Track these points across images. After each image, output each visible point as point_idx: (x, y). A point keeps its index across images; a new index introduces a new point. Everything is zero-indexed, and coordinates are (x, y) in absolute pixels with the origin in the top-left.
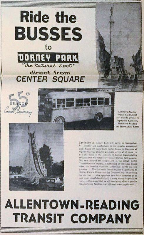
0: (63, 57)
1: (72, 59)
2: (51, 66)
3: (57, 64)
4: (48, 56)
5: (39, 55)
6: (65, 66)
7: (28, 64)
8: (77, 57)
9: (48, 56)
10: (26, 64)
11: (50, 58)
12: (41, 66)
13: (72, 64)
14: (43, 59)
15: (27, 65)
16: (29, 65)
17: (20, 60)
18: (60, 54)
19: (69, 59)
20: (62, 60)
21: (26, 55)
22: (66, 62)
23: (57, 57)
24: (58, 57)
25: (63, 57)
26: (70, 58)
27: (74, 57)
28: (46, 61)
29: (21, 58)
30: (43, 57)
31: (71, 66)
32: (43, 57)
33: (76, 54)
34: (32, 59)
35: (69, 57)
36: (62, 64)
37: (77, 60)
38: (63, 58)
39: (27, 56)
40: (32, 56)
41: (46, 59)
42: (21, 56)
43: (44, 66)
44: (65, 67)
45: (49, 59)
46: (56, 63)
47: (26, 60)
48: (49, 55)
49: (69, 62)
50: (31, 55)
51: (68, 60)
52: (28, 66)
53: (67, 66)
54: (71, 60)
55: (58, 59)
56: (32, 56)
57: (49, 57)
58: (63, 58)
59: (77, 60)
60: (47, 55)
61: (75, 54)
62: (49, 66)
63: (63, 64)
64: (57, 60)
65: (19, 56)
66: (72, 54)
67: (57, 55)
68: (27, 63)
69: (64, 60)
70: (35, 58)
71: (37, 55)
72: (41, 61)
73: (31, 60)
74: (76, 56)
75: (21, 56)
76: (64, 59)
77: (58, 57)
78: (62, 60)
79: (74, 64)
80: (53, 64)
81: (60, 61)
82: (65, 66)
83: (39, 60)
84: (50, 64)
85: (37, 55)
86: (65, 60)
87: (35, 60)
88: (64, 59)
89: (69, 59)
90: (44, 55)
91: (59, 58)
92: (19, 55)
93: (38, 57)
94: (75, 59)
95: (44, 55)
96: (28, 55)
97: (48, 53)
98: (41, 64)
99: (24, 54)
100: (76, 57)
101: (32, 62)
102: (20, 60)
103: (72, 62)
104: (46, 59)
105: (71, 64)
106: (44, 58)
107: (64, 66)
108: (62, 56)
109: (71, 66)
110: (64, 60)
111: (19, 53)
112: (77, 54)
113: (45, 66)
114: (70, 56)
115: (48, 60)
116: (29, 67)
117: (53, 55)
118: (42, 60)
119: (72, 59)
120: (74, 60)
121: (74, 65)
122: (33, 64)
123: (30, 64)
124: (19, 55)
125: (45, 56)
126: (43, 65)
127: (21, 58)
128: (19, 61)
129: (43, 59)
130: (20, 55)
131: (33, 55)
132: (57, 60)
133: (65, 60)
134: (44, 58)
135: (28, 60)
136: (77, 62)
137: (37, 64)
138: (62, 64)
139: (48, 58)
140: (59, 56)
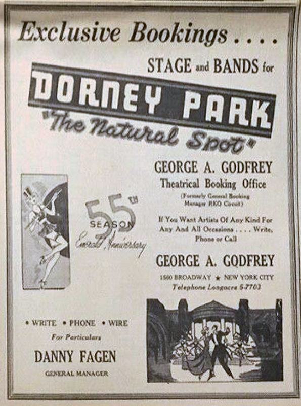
0: (215, 104)
1: (248, 116)
2: (159, 139)
3: (185, 134)
4: (153, 95)
5: (116, 86)
6: (213, 144)
7: (66, 115)
8: (270, 112)
9: (153, 95)
10: (59, 116)
12: (119, 130)
13: (247, 138)
14: (132, 103)
16: (69, 122)
17: (38, 95)
18: (205, 92)
19: (237, 117)
20: (208, 118)
21: (63, 79)
22: (224, 125)
24: (193, 101)
25: (215, 104)
26: (242, 112)
27: (259, 111)
29: (43, 91)
30: (133, 93)
32: (133, 93)
33: (266, 101)
34: (87, 96)
35: (238, 106)
36: (204, 135)
38: (215, 108)
40: (88, 87)
41: (142, 105)
42: (44, 81)
44: (213, 148)
46: (180, 129)
47: (61, 98)
48: (159, 90)
50: (84, 82)
51: (232, 121)
54: (243, 122)
55: (191, 110)
56: (88, 87)
57: (157, 100)
58: (215, 108)
60: (149, 89)
62: (153, 136)
63: (211, 134)
64: (186, 115)
66: (250, 97)
67: (189, 95)
68: (62, 112)
69: (214, 119)
70: (99, 96)
72: (121, 111)
73: (82, 101)
74: (266, 105)
75: (44, 81)
76: (214, 114)
77: (193, 101)
78: (208, 118)
80: (167, 129)
82: (213, 144)
83: (115, 105)
84: (155, 127)
85: (107, 85)
86: (219, 119)
88: (214, 114)
89: (237, 117)
90: (136, 88)
91: (197, 105)
93: (111, 90)
94: (259, 120)
96: (71, 81)
97: (154, 83)
98: (120, 125)
101: (87, 108)
103: (248, 130)
104: (142, 105)
105: (244, 136)
106: (135, 98)
108: (211, 99)
109: (238, 147)
110: (214, 119)
113: (133, 132)
114: (243, 103)
115: (151, 110)
116: (67, 128)
117: (173, 94)
119: (248, 116)
120: (254, 124)
121: (252, 143)
122: (86, 118)
123: (74, 117)
125: (141, 94)
127: (43, 91)
128: (33, 101)
129: (132, 103)
130: (39, 76)
131: (93, 83)
132: (186, 115)
133: (219, 119)
134: (135, 98)
135: (68, 98)
136: (267, 133)
137: (105, 122)
138: (204, 135)
139: (153, 102)
140: (198, 97)
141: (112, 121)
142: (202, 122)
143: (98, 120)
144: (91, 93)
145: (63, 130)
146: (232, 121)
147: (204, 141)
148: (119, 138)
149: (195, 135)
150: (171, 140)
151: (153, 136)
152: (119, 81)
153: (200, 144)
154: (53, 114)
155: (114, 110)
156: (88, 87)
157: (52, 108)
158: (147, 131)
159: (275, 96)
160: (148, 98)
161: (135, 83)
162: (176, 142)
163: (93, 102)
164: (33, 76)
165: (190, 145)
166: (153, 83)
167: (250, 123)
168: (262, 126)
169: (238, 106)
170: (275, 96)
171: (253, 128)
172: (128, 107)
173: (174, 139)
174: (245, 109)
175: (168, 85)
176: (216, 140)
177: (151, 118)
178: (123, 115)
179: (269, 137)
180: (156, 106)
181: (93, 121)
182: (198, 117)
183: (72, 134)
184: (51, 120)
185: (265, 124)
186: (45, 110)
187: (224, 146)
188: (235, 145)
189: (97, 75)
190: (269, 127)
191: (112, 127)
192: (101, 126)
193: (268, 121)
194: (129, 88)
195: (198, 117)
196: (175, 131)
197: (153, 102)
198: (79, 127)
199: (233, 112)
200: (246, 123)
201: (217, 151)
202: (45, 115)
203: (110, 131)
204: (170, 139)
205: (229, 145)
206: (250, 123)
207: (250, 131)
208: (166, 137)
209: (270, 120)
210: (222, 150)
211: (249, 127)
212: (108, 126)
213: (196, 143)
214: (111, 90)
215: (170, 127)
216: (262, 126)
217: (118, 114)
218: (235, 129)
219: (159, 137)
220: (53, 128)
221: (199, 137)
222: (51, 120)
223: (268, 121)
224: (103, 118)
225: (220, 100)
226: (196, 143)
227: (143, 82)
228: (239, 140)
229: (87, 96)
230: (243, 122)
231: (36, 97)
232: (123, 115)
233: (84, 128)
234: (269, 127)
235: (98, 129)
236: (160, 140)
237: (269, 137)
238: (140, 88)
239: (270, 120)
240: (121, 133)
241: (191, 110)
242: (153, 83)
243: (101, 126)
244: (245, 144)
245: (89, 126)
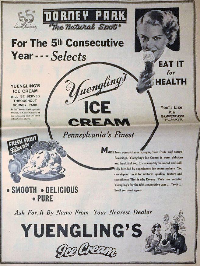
0: (106, 14)
1: (118, 17)
3: (97, 25)
4: (85, 13)
5: (73, 12)
6: (107, 28)
7: (57, 25)
8: (125, 15)
9: (85, 13)
10: (55, 25)
12: (75, 27)
13: (118, 24)
14: (79, 17)
15: (55, 27)
17: (47, 19)
18: (102, 10)
19: (114, 17)
20: (105, 19)
21: (54, 13)
22: (110, 21)
23: (98, 14)
24: (99, 14)
25: (106, 14)
26: (116, 16)
27: (121, 15)
29: (48, 18)
30: (79, 14)
31: (115, 28)
32: (79, 14)
34: (63, 17)
35: (114, 14)
38: (106, 15)
39: (56, 14)
40: (63, 14)
41: (82, 17)
42: (48, 14)
43: (78, 28)
44: (107, 29)
45: (87, 17)
46: (96, 24)
47: (55, 19)
48: (87, 12)
49: (114, 21)
50: (62, 13)
51: (112, 19)
52: (57, 28)
53: (111, 28)
54: (116, 19)
55: (99, 17)
56: (63, 14)
57: (87, 15)
58: (106, 15)
60: (84, 12)
62: (87, 27)
63: (106, 24)
64: (97, 19)
66: (118, 10)
67: (97, 12)
69: (106, 19)
70: (67, 17)
73: (62, 19)
74: (123, 12)
75: (48, 14)
76: (106, 17)
77: (99, 14)
78: (105, 19)
79: (120, 24)
80: (91, 24)
82: (107, 28)
83: (73, 19)
84: (87, 24)
85: (70, 13)
86: (108, 19)
89: (114, 17)
90: (79, 12)
91: (100, 15)
92: (45, 13)
93: (71, 14)
94: (122, 17)
95: (79, 12)
96: (57, 13)
97: (85, 9)
98: (75, 25)
99: (52, 11)
101: (64, 21)
103: (118, 21)
104: (82, 17)
105: (117, 24)
106: (79, 15)
107: (106, 27)
108: (105, 12)
109: (115, 28)
110: (106, 19)
113: (80, 27)
114: (116, 12)
115: (85, 19)
117: (92, 12)
119: (118, 17)
120: (120, 19)
121: (120, 26)
122: (64, 25)
123: (60, 25)
126: (77, 25)
127: (48, 18)
128: (45, 21)
129: (79, 17)
131: (65, 12)
132: (97, 19)
134: (79, 15)
135: (57, 19)
136: (125, 22)
137: (70, 25)
138: (104, 25)
139: (85, 16)
140: (100, 12)
141: (72, 24)
143: (68, 25)
145: (56, 30)
146: (112, 19)
147: (104, 27)
148: (75, 30)
149: (100, 25)
150: (93, 28)
151: (87, 27)
153: (102, 28)
154: (52, 25)
155: (73, 21)
156: (63, 15)
157: (52, 23)
158: (85, 26)
159: (126, 9)
162: (94, 28)
163: (66, 19)
165: (99, 29)
167: (119, 19)
168: (123, 19)
169: (114, 14)
170: (126, 9)
171: (120, 21)
172: (77, 19)
173: (94, 27)
176: (108, 26)
177: (86, 21)
178: (75, 22)
179: (126, 23)
181: (66, 25)
182: (101, 19)
183: (59, 31)
184: (52, 27)
185: (124, 19)
186: (49, 24)
187: (111, 28)
188: (114, 27)
189: (66, 10)
190: (125, 20)
191: (73, 26)
192: (69, 27)
193: (125, 18)
194: (77, 12)
195: (101, 19)
196: (94, 25)
198: (61, 28)
200: (117, 19)
201: (108, 30)
202: (50, 26)
203: (72, 28)
204: (92, 27)
205: (112, 27)
206: (119, 19)
207: (119, 22)
208: (91, 27)
209: (126, 17)
210: (110, 29)
211: (119, 20)
212: (71, 26)
213: (101, 28)
214: (71, 14)
215: (93, 23)
216: (123, 19)
217: (74, 22)
219: (89, 27)
220: (53, 30)
221: (102, 26)
222: (52, 27)
223: (125, 18)
224: (69, 24)
225: (108, 12)
226: (101, 28)
227: (81, 10)
228: (115, 25)
229: (63, 17)
230: (116, 19)
231: (46, 20)
232: (75, 22)
233: (63, 28)
234: (125, 20)
235: (68, 28)
236: (89, 28)
237: (126, 23)
238: (81, 12)
239: (126, 17)
240: (76, 28)
241: (99, 17)
243: (69, 27)
244: (118, 26)
245: (65, 27)
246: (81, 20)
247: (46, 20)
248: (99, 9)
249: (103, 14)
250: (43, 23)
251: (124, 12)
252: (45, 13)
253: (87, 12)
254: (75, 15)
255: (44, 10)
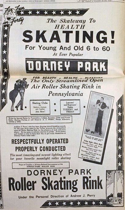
0: (88, 65)
1: (99, 68)
4: (67, 64)
5: (55, 63)
8: (106, 65)
9: (67, 64)
11: (69, 66)
14: (61, 68)
17: (30, 69)
18: (84, 61)
19: (95, 69)
20: (86, 70)
21: (37, 62)
23: (80, 65)
24: (80, 65)
25: (88, 65)
26: (97, 67)
27: (102, 66)
28: (64, 71)
30: (61, 64)
32: (61, 64)
34: (46, 67)
37: (105, 70)
38: (88, 67)
39: (38, 64)
40: (46, 64)
42: (31, 64)
47: (37, 69)
48: (69, 62)
51: (94, 70)
56: (46, 64)
57: (69, 66)
58: (88, 67)
59: (105, 70)
60: (66, 62)
61: (103, 61)
64: (79, 70)
65: (28, 63)
66: (99, 61)
67: (79, 63)
69: (88, 70)
70: (50, 67)
71: (52, 63)
73: (44, 69)
74: (104, 63)
75: (31, 64)
77: (80, 65)
78: (86, 70)
81: (83, 71)
83: (55, 69)
85: (52, 63)
86: (90, 70)
87: (49, 70)
89: (95, 69)
90: (61, 62)
91: (82, 66)
92: (28, 62)
93: (53, 64)
94: (102, 68)
95: (61, 62)
96: (39, 63)
97: (67, 60)
99: (34, 60)
100: (104, 65)
102: (30, 69)
104: (64, 68)
106: (61, 66)
108: (86, 63)
110: (88, 70)
111: (27, 59)
112: (106, 62)
114: (97, 63)
115: (67, 70)
117: (74, 63)
118: (60, 69)
119: (99, 68)
120: (101, 70)
124: (28, 62)
125: (63, 64)
127: (31, 67)
129: (61, 68)
130: (29, 62)
131: (47, 63)
132: (79, 70)
133: (90, 70)
134: (61, 66)
136: (106, 73)
139: (67, 67)
140: (82, 63)
142: (84, 72)
144: (47, 66)
146: (94, 70)
152: (55, 61)
155: (55, 71)
160: (66, 66)
161: (61, 61)
163: (48, 69)
164: (27, 63)
166: (67, 60)
168: (104, 71)
170: (107, 60)
171: (101, 72)
174: (97, 65)
175: (72, 60)
180: (69, 68)
185: (105, 70)
194: (59, 63)
197: (67, 67)
199: (94, 67)
209: (106, 68)
211: (100, 71)
214: (53, 64)
216: (104, 71)
218: (95, 73)
225: (89, 63)
227: (63, 60)
229: (46, 67)
237: (107, 74)
239: (106, 68)
242: (67, 60)
246: (63, 71)
247: (29, 70)
248: (81, 60)
249: (84, 65)
250: (27, 73)
251: (105, 63)
252: (27, 63)
253: (69, 62)
254: (57, 66)
255: (26, 60)
